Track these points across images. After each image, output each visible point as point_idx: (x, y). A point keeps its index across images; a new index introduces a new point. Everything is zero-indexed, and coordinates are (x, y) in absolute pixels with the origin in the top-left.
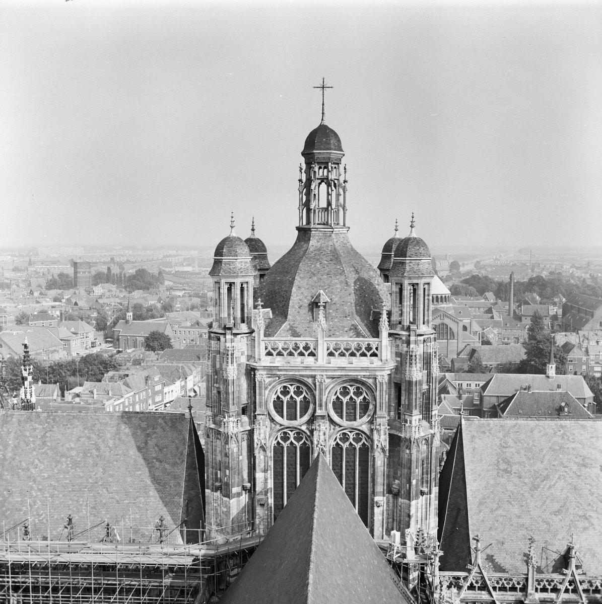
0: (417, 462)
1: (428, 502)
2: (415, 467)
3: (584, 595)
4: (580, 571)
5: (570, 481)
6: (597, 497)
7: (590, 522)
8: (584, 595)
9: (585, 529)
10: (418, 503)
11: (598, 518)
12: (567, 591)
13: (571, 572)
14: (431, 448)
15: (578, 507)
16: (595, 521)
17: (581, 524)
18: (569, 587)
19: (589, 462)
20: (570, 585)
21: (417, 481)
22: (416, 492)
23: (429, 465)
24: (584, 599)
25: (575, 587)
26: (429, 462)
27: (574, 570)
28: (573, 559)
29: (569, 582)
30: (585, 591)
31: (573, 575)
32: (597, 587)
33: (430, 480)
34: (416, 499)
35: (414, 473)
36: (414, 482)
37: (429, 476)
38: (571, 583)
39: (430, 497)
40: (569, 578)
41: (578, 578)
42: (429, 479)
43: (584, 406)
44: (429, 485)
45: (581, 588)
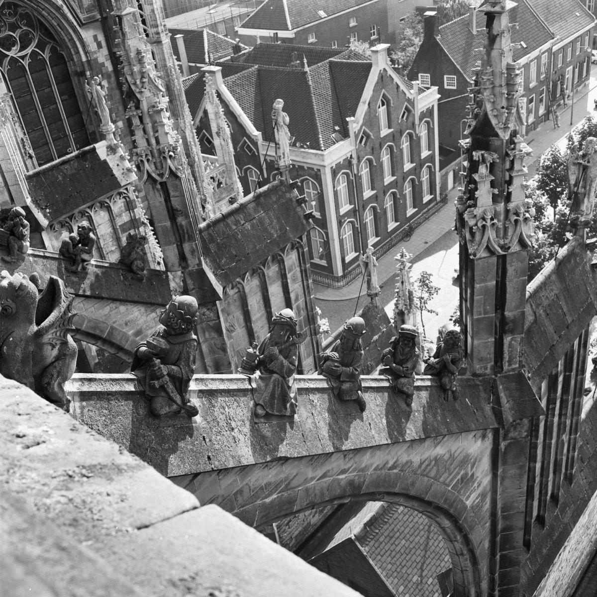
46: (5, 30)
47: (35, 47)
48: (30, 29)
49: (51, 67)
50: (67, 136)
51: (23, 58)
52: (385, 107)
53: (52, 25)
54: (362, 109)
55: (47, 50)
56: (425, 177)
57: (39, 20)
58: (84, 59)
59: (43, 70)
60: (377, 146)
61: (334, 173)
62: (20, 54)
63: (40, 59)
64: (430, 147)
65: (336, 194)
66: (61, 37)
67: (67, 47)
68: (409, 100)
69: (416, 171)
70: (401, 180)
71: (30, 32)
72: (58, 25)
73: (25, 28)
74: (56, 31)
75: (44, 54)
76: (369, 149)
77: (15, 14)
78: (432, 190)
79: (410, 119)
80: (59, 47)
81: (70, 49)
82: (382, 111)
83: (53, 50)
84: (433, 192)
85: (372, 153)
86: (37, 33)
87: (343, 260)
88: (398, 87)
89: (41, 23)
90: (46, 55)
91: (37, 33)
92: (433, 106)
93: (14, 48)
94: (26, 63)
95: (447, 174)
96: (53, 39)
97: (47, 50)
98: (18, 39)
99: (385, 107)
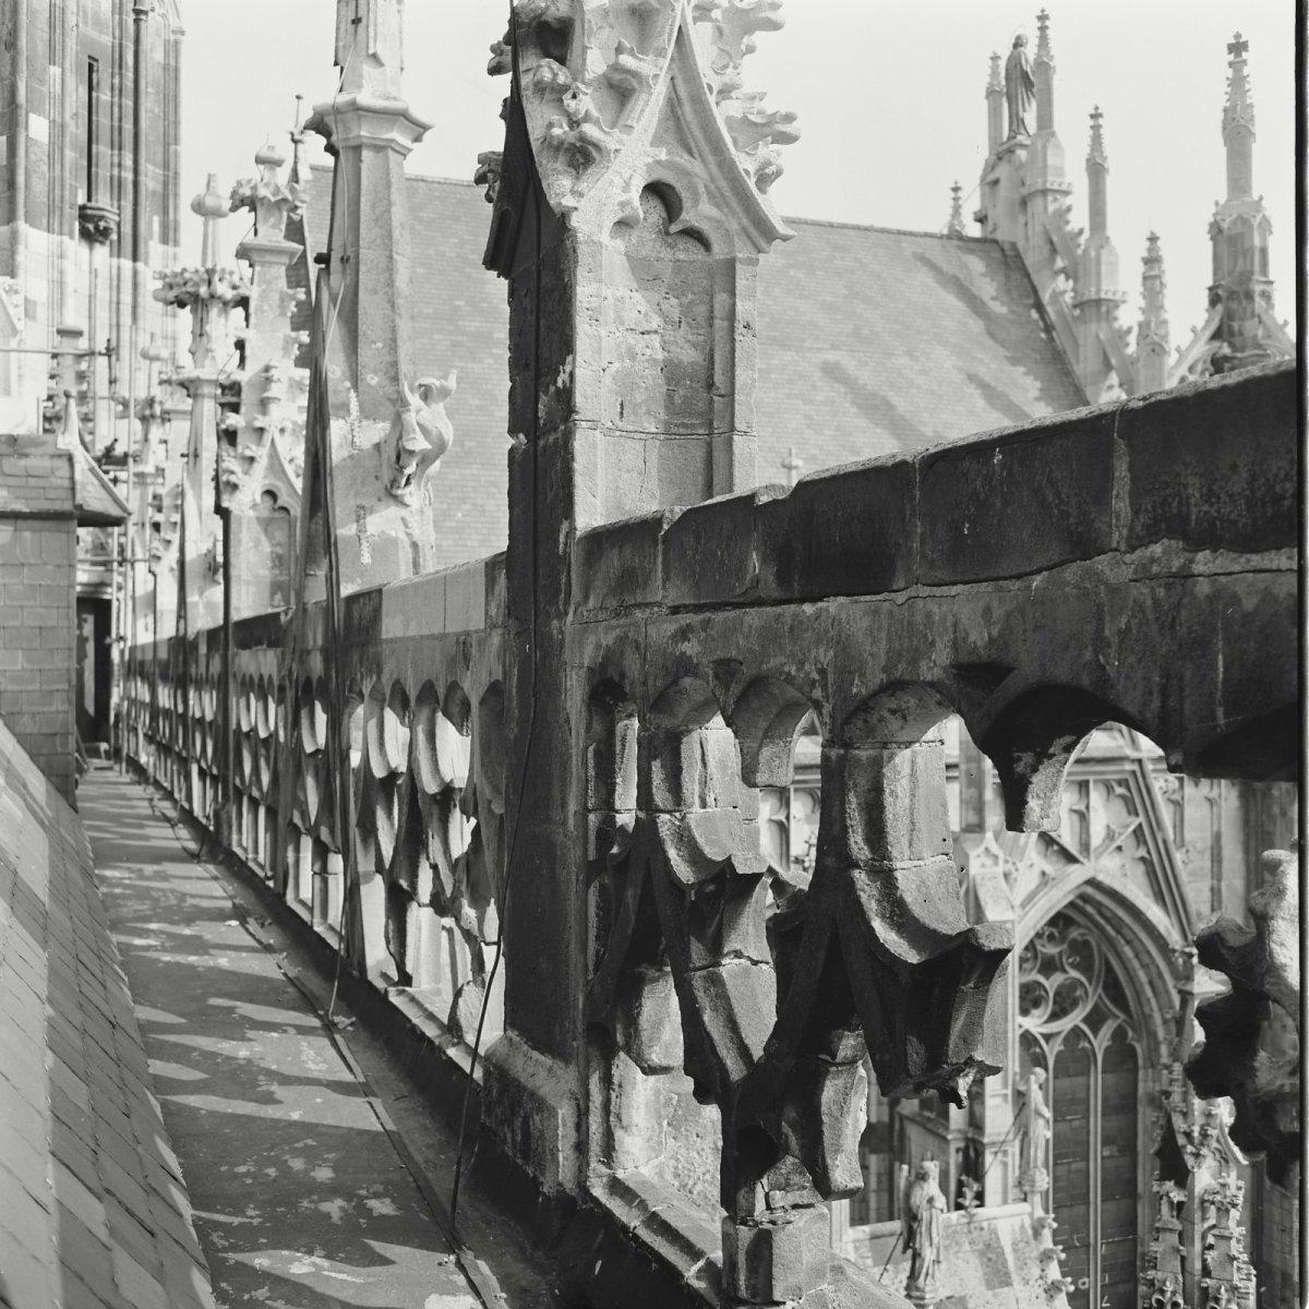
0: (52, 27)
1: (127, 298)
2: (42, 49)
10: (61, 256)
14: (137, 21)
21: (58, 129)
22: (51, 190)
23: (129, 103)
26: (129, 83)
33: (136, 184)
34: (49, 230)
35: (38, 77)
36: (37, 127)
37: (128, 161)
39: (135, 274)
42: (128, 176)
44: (128, 205)
46: (1032, 969)
47: (1085, 1020)
48: (1084, 980)
49: (1103, 1072)
50: (1088, 1246)
51: (1048, 1037)
53: (1132, 979)
55: (1107, 1030)
57: (1108, 963)
59: (1083, 1075)
62: (1047, 1029)
63: (1084, 1049)
66: (1147, 1010)
67: (1152, 1035)
71: (1082, 983)
72: (1151, 983)
73: (1074, 974)
74: (1138, 993)
75: (1095, 1037)
77: (1062, 940)
80: (1134, 1030)
81: (1157, 1044)
83: (1119, 1034)
86: (1097, 986)
89: (1109, 969)
90: (1101, 1042)
91: (1097, 986)
93: (1035, 1012)
94: (1051, 1051)
96: (1125, 1008)
97: (1107, 1030)
98: (1051, 995)
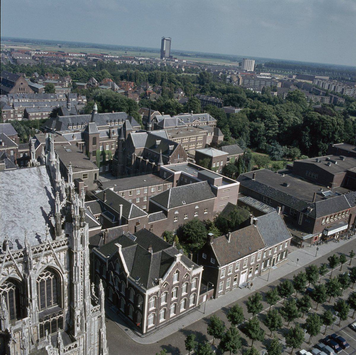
3: (15, 260)
4: (12, 250)
5: (3, 204)
6: (17, 210)
7: (15, 223)
8: (15, 260)
9: (13, 227)
11: (19, 220)
12: (6, 261)
13: (8, 252)
15: (8, 217)
16: (17, 222)
17: (10, 225)
18: (7, 259)
19: (12, 192)
20: (8, 258)
24: (15, 262)
25: (10, 258)
27: (9, 250)
28: (8, 245)
29: (7, 256)
30: (16, 258)
31: (9, 252)
32: (21, 254)
38: (8, 257)
40: (7, 254)
41: (11, 253)
43: (13, 140)
45: (13, 258)
52: (177, 273)
54: (167, 275)
56: (192, 297)
58: (62, 281)
60: (171, 287)
61: (149, 297)
64: (197, 286)
65: (149, 304)
68: (188, 272)
69: (188, 296)
70: (180, 299)
73: (48, 272)
76: (167, 288)
78: (194, 302)
79: (188, 278)
82: (176, 275)
84: (195, 303)
85: (168, 290)
87: (147, 327)
88: (184, 267)
90: (52, 278)
92: (200, 273)
95: (203, 296)
99: (177, 273)
